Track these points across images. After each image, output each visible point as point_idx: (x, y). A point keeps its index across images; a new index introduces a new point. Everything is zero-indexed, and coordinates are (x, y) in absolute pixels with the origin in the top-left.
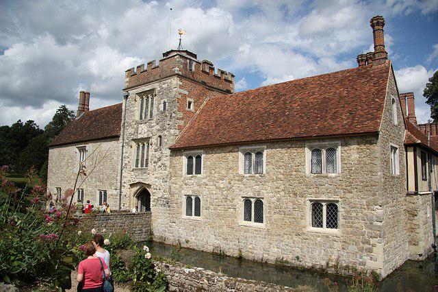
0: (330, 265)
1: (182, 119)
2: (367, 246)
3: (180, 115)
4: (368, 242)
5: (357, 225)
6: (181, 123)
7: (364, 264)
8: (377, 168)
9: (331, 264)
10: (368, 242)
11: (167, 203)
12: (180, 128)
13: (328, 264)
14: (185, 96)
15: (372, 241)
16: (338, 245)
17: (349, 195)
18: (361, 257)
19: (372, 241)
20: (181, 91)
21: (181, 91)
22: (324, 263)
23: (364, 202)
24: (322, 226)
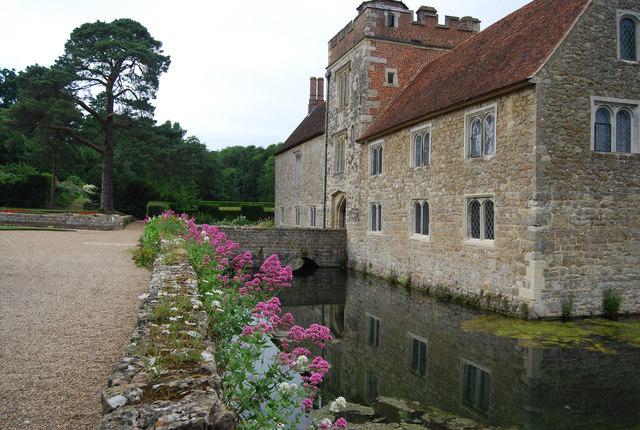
0: (484, 294)
1: (377, 99)
2: (519, 264)
3: (373, 93)
4: (520, 259)
5: (510, 232)
6: (376, 105)
7: (515, 292)
8: (533, 141)
9: (486, 292)
10: (520, 259)
11: (357, 218)
12: (373, 112)
13: (482, 292)
14: (382, 66)
15: (529, 256)
16: (492, 264)
17: (503, 187)
18: (514, 282)
19: (529, 256)
20: (376, 59)
21: (376, 59)
22: (478, 291)
23: (517, 195)
24: (478, 237)
